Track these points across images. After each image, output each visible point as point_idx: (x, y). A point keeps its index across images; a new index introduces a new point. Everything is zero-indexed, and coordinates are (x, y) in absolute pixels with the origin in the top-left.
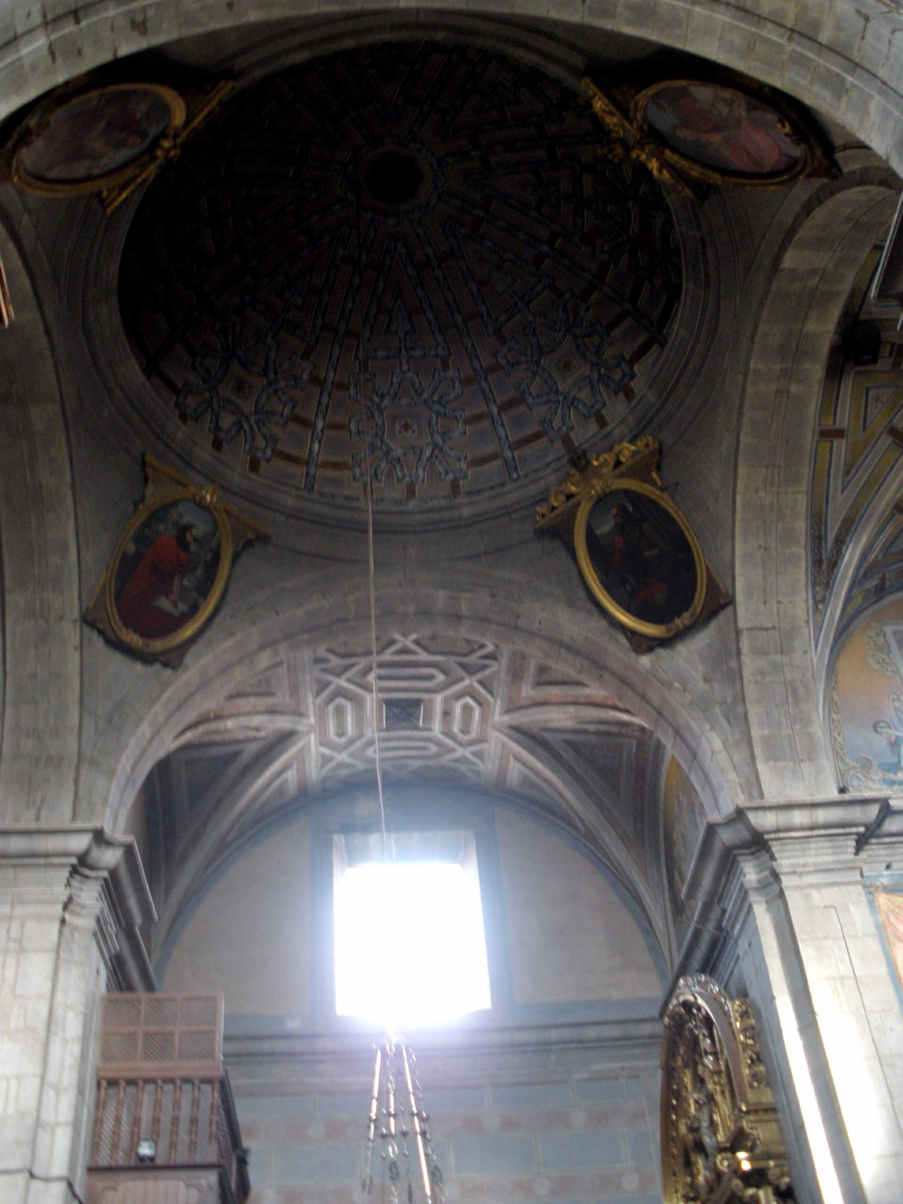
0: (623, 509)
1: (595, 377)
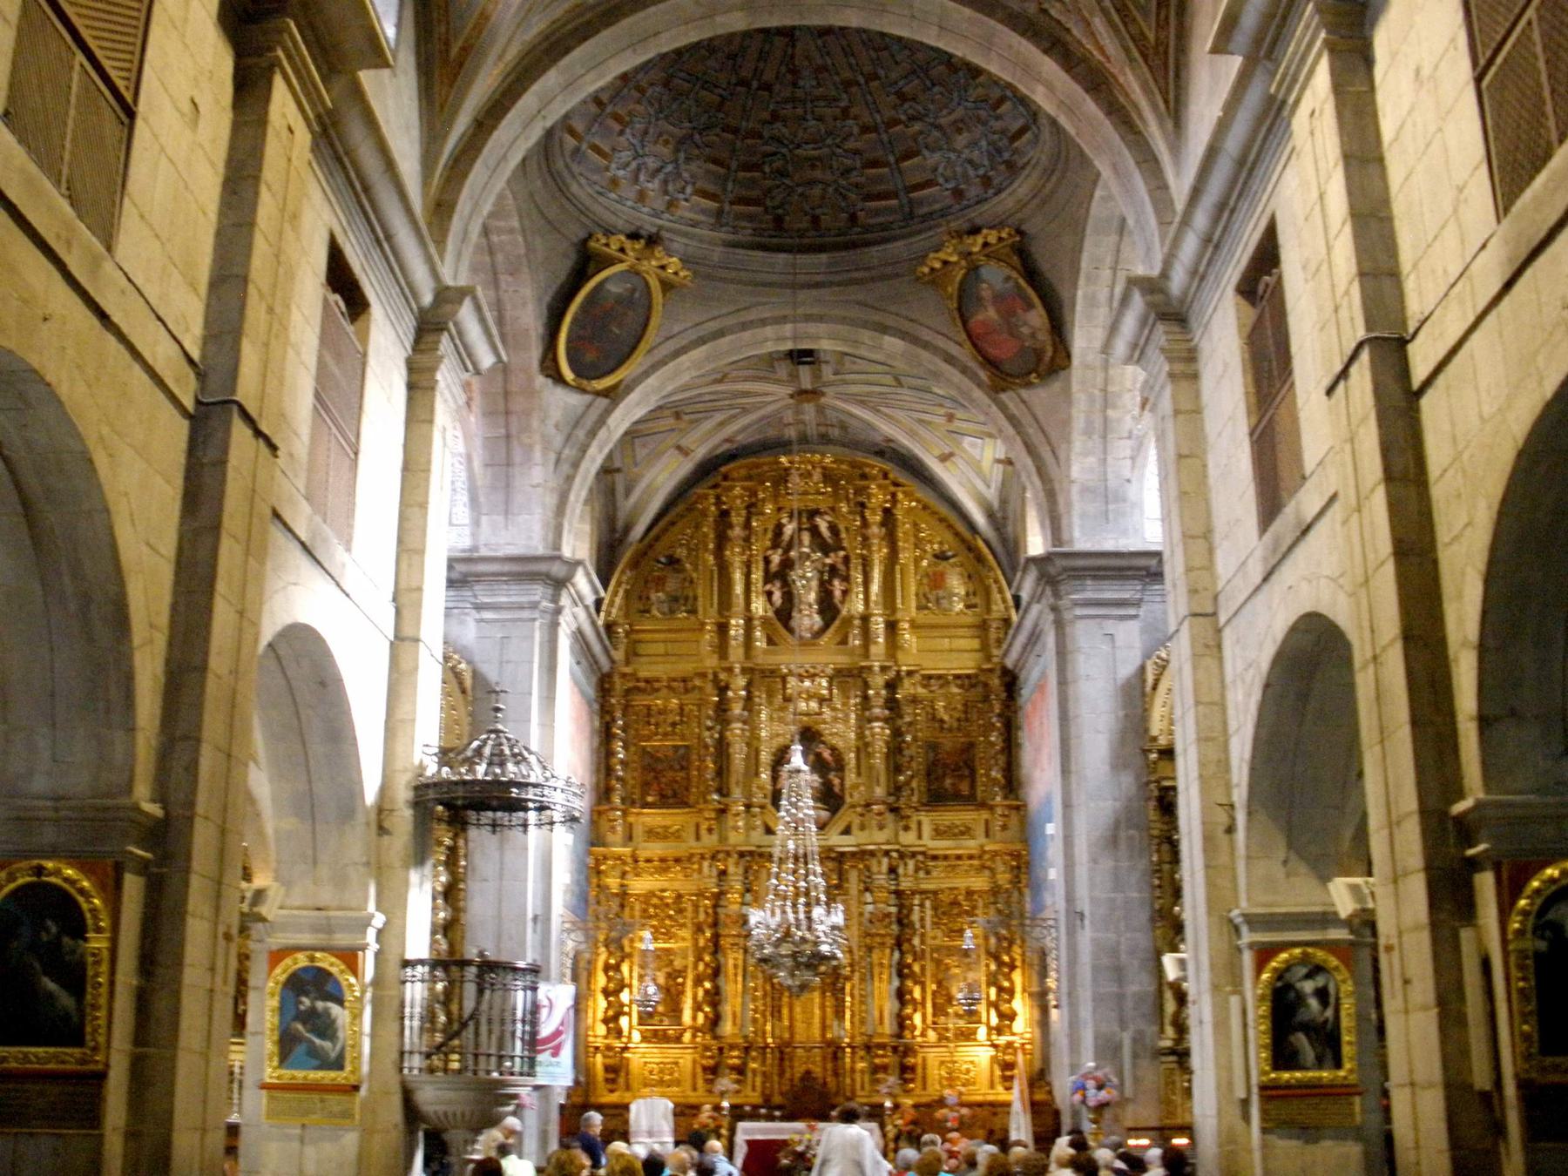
0: (634, 290)
1: (670, 168)
